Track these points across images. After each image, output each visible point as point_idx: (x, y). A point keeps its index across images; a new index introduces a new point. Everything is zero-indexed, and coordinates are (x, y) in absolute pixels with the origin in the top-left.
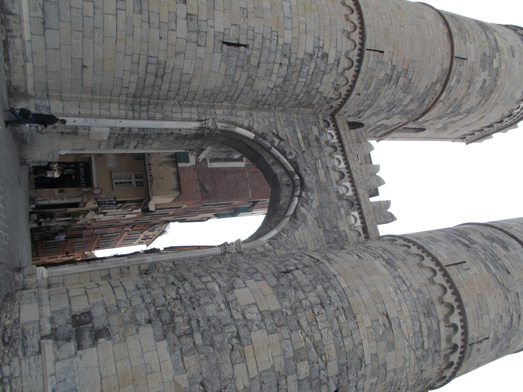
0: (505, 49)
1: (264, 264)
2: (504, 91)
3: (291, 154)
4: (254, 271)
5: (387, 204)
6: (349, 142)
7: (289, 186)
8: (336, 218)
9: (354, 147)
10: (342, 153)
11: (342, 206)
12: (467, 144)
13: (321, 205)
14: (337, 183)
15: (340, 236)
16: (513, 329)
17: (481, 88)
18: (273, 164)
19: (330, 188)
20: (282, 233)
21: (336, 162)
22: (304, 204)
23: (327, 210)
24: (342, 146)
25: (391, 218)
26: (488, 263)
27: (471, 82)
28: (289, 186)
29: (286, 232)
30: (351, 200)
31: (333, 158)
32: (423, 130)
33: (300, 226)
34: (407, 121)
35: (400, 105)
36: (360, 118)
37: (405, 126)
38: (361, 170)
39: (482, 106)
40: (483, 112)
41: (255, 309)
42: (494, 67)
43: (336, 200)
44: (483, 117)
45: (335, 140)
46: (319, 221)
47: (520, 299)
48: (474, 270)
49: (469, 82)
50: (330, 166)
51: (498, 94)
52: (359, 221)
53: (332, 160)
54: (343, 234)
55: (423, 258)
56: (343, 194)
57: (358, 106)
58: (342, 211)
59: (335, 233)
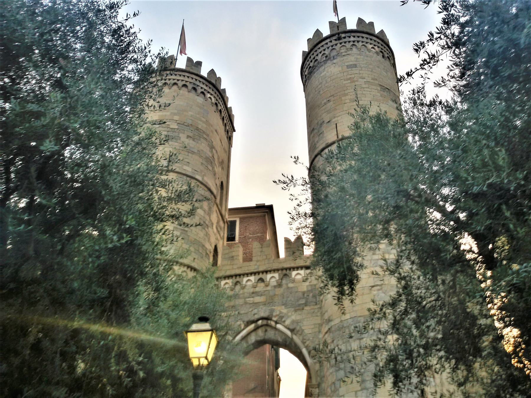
1: (329, 375)
2: (197, 116)
3: (240, 325)
4: (333, 386)
5: (287, 241)
6: (233, 269)
7: (266, 331)
8: (297, 292)
9: (237, 264)
10: (242, 276)
11: (287, 284)
12: (234, 131)
13: (285, 304)
14: (267, 286)
15: (311, 291)
17: (194, 140)
18: (247, 342)
19: (271, 293)
20: (306, 344)
21: (249, 283)
22: (283, 320)
23: (289, 299)
24: (236, 276)
28: (266, 331)
29: (305, 341)
30: (282, 276)
31: (246, 285)
32: (222, 183)
33: (300, 327)
34: (215, 206)
35: (204, 217)
36: (211, 252)
37: (219, 206)
38: (258, 261)
39: (208, 135)
40: (212, 132)
42: (177, 127)
44: (216, 131)
45: (230, 281)
46: (299, 308)
49: (188, 152)
50: (252, 290)
51: (199, 122)
52: (300, 272)
53: (247, 287)
54: (310, 288)
56: (277, 282)
57: (202, 258)
58: (291, 285)
59: (308, 296)
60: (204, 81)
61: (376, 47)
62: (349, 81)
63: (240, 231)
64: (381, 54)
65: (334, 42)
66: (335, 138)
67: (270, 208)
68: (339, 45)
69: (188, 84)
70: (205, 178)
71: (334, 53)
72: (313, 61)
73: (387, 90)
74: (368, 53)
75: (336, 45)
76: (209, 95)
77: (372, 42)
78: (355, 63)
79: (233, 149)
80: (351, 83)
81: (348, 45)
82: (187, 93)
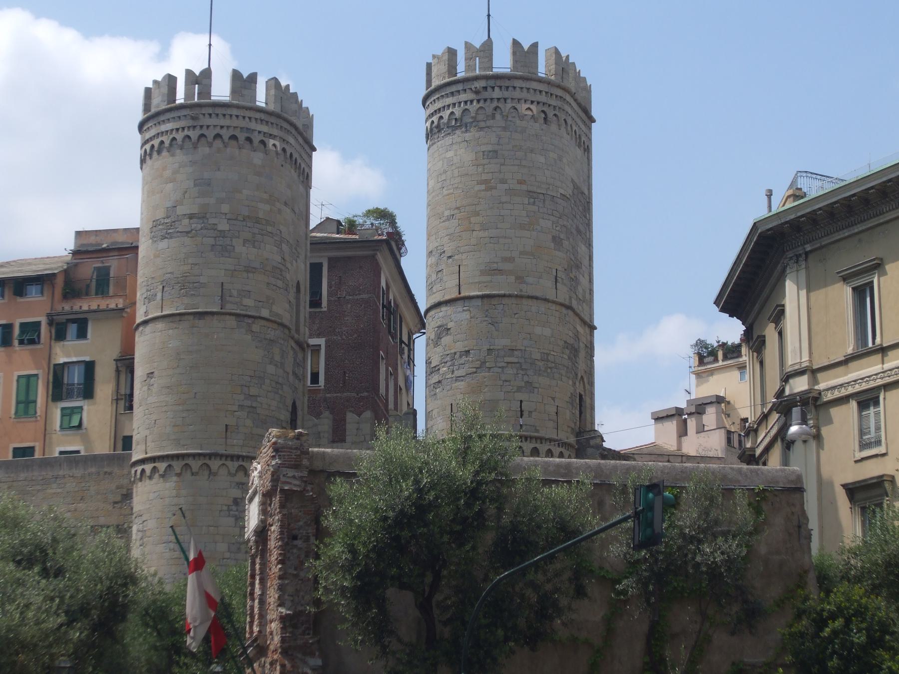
16: (522, 360)
26: (457, 373)
27: (249, 269)
40: (280, 210)
47: (496, 347)
49: (248, 272)
60: (263, 116)
62: (483, 187)
64: (543, 116)
66: (454, 295)
68: (475, 103)
69: (237, 133)
70: (275, 308)
73: (541, 196)
74: (518, 122)
75: (472, 102)
76: (272, 142)
78: (496, 147)
80: (486, 190)
81: (489, 107)
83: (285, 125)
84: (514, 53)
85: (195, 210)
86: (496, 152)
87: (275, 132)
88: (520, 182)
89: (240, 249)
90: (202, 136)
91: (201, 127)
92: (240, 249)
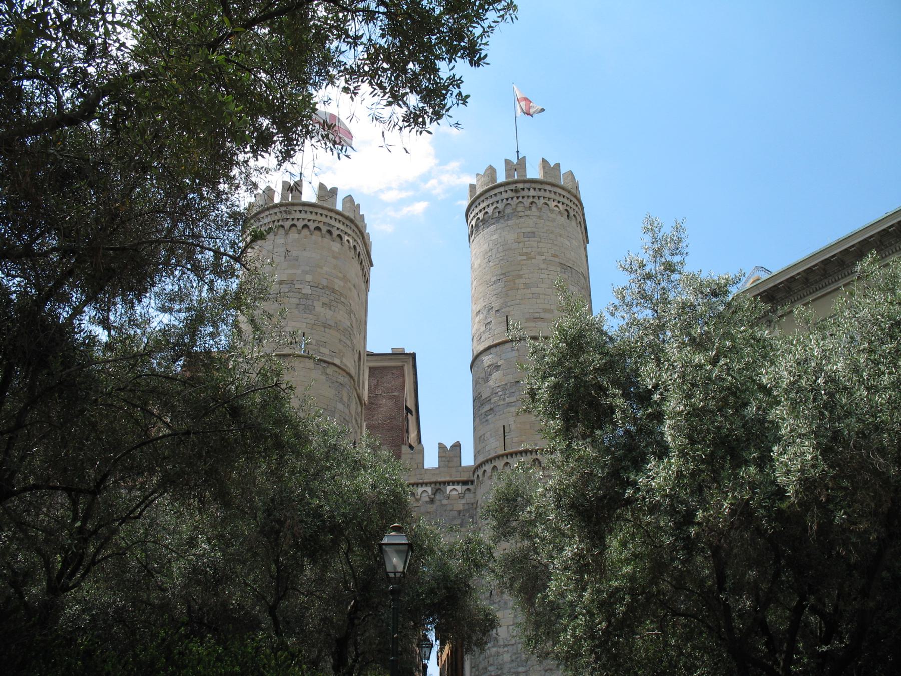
0: (290, 271)
5: (442, 447)
12: (372, 265)
15: (467, 510)
25: (457, 446)
27: (326, 326)
40: (350, 289)
41: (511, 628)
42: (309, 292)
43: (435, 506)
48: (511, 420)
49: (325, 327)
51: (336, 281)
54: (466, 507)
55: (495, 466)
58: (445, 502)
60: (341, 218)
61: (560, 205)
62: (525, 257)
63: (370, 386)
65: (510, 194)
67: (413, 355)
68: (515, 199)
69: (321, 226)
70: (344, 360)
71: (508, 211)
72: (483, 212)
74: (549, 214)
75: (512, 198)
76: (346, 238)
77: (557, 198)
79: (371, 295)
80: (527, 260)
81: (527, 202)
82: (320, 239)
83: (356, 230)
84: (544, 167)
85: (284, 278)
86: (533, 233)
87: (350, 232)
88: (554, 256)
89: (319, 309)
90: (294, 225)
91: (293, 219)
92: (319, 309)
